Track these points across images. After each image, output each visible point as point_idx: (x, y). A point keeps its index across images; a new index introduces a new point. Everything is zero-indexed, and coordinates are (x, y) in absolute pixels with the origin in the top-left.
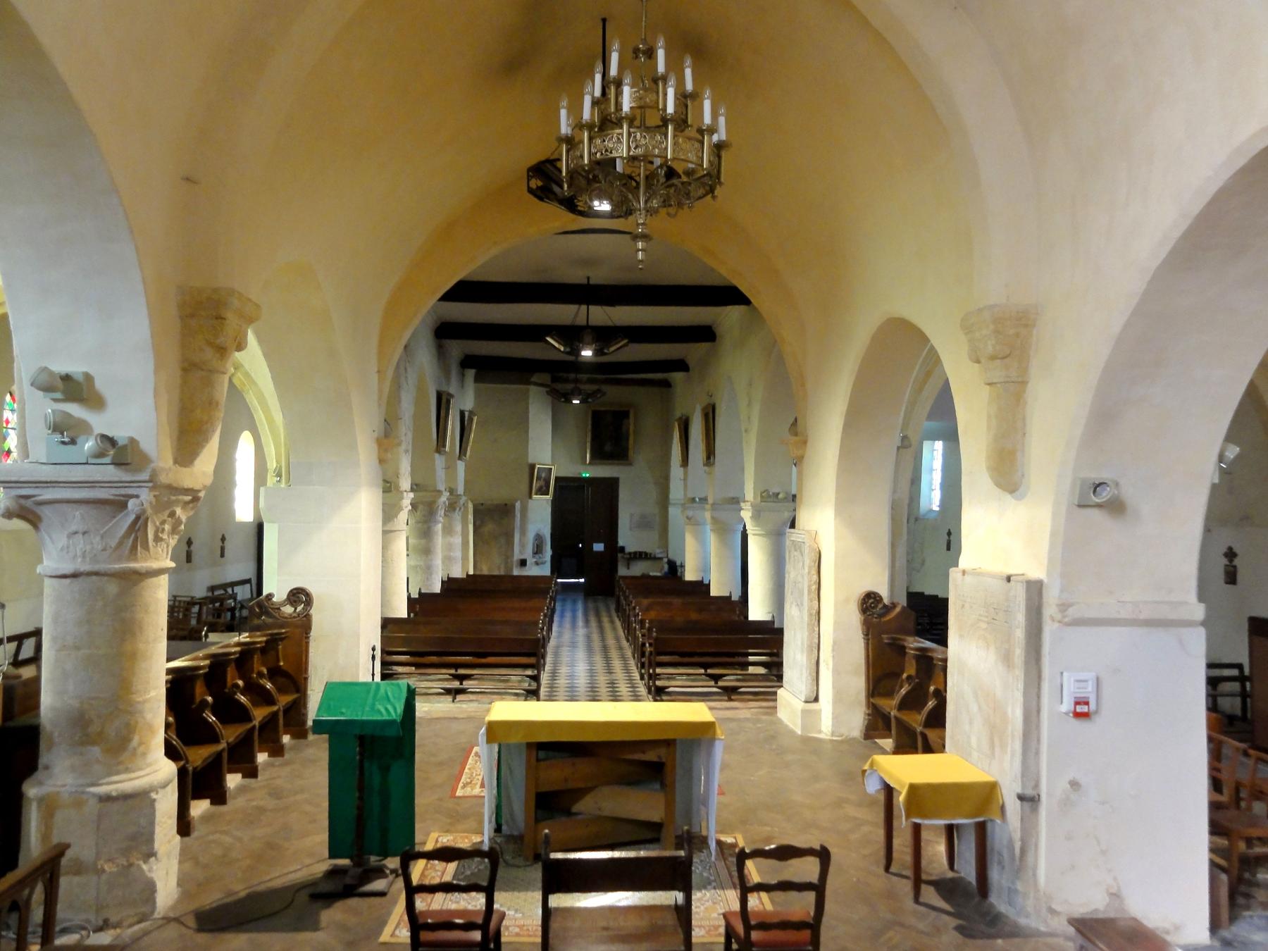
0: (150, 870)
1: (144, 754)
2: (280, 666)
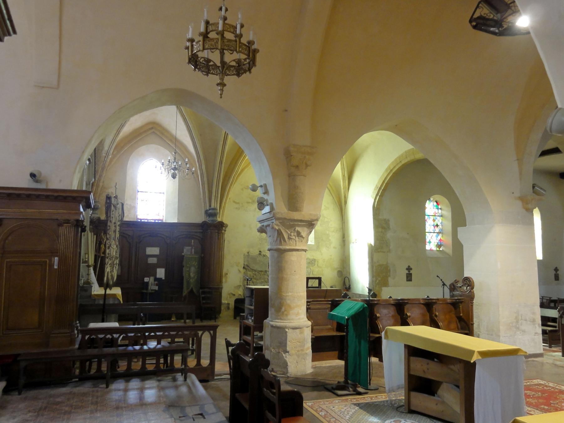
0: (286, 357)
1: (287, 315)
2: (461, 316)
